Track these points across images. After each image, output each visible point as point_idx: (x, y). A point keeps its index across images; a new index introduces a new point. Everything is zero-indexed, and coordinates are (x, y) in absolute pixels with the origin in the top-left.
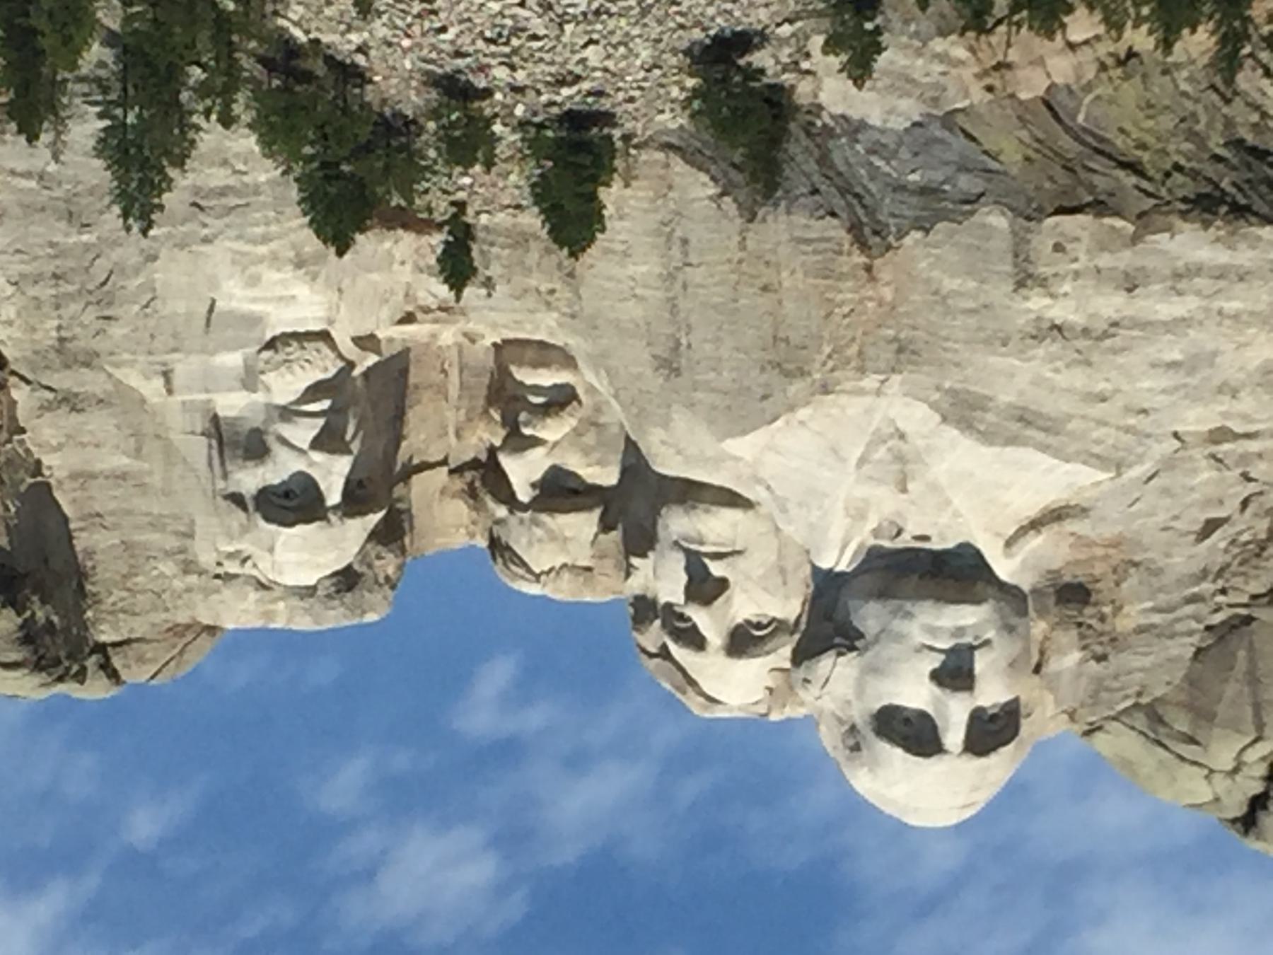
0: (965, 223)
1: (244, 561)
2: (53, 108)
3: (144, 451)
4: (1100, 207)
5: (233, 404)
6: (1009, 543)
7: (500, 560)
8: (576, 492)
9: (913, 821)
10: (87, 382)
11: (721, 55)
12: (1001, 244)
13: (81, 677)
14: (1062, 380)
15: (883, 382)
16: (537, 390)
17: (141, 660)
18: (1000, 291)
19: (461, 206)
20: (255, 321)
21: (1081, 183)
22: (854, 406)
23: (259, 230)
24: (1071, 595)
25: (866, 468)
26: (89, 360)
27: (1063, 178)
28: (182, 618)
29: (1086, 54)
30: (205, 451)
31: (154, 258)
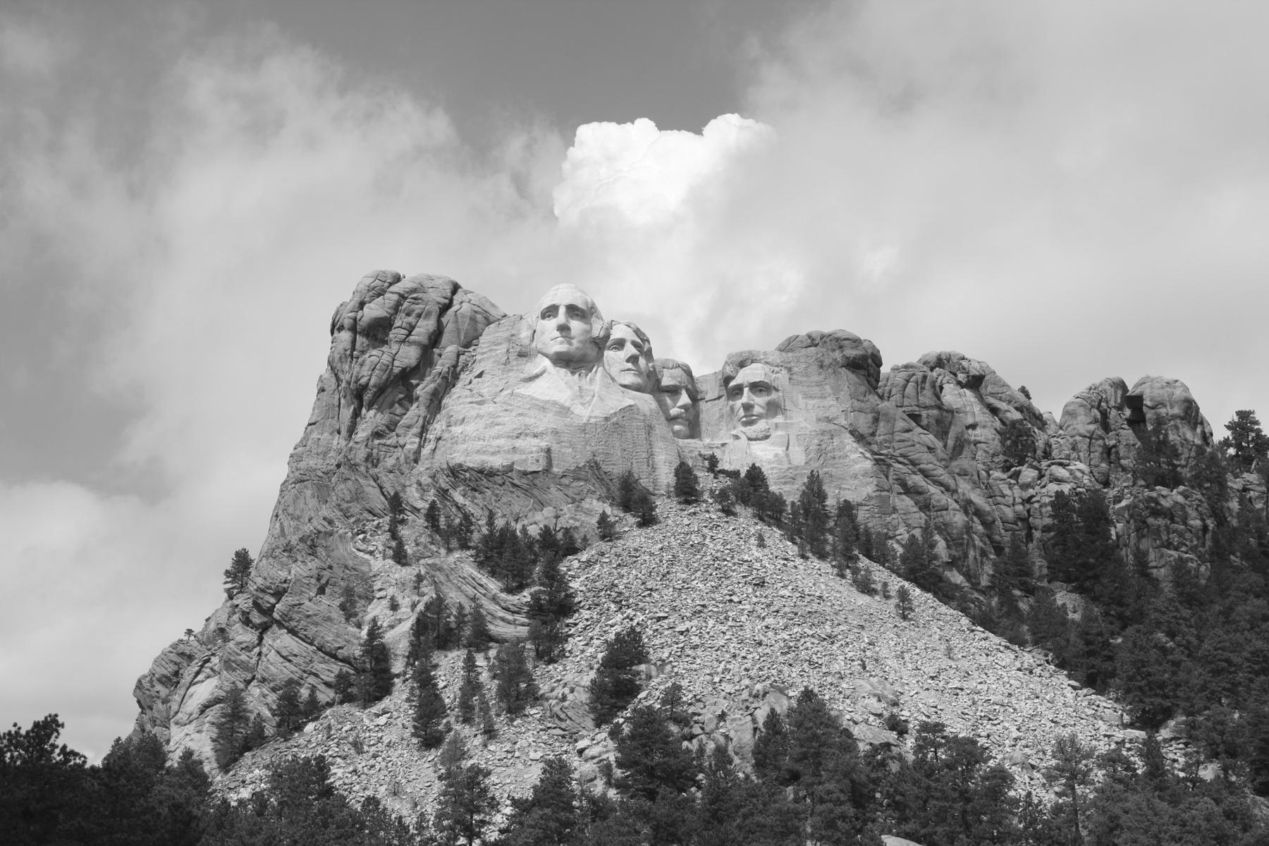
2: (839, 508)
4: (525, 474)
5: (779, 419)
6: (544, 372)
10: (824, 426)
11: (647, 521)
12: (555, 462)
13: (822, 337)
14: (533, 421)
18: (555, 447)
19: (715, 478)
20: (773, 444)
22: (597, 413)
24: (522, 355)
26: (823, 433)
27: (537, 482)
28: (790, 354)
29: (531, 520)
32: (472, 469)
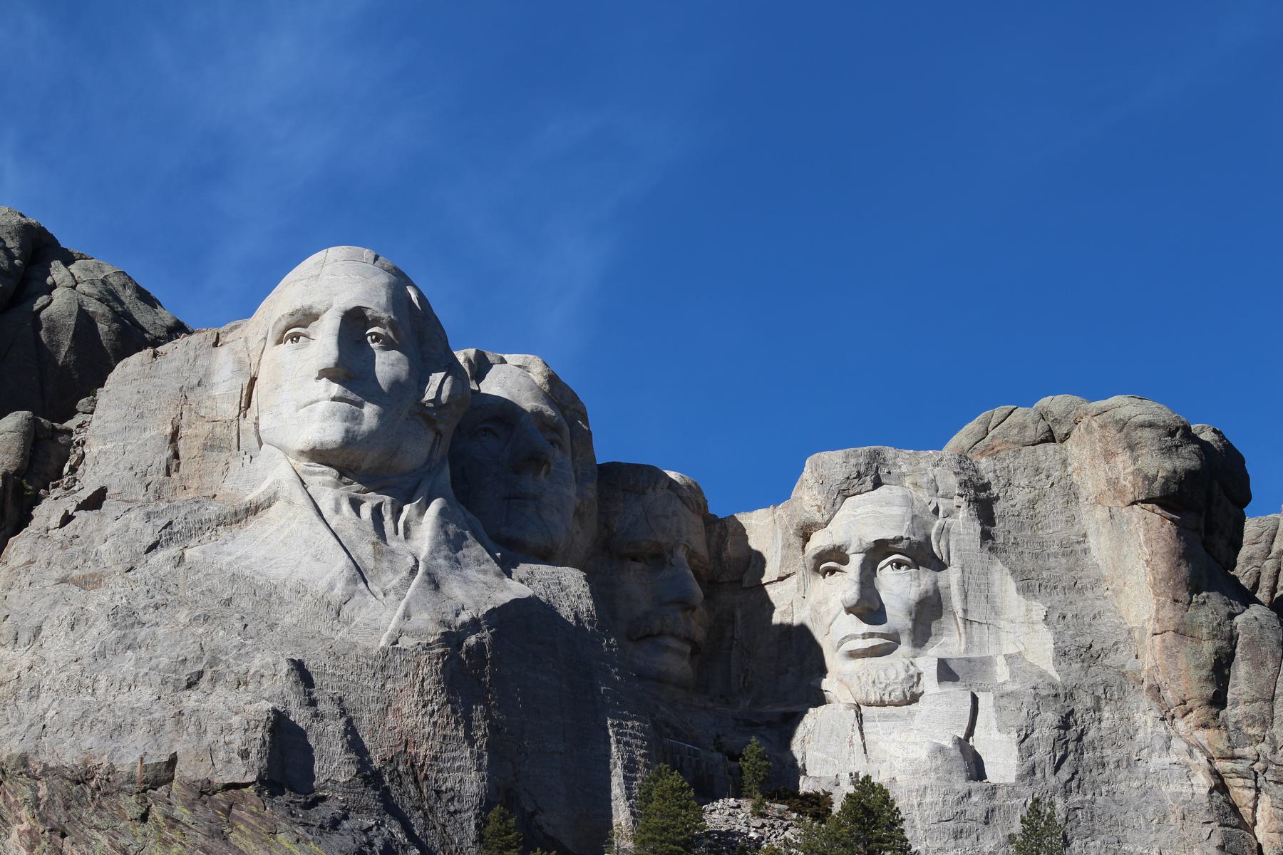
0: (322, 780)
1: (936, 511)
3: (1023, 609)
4: (205, 791)
7: (701, 501)
8: (634, 559)
9: (368, 254)
15: (397, 642)
16: (667, 648)
17: (1023, 427)
21: (223, 810)
23: (928, 799)
25: (411, 562)
30: (971, 606)
31: (1021, 778)
32: (57, 772)
